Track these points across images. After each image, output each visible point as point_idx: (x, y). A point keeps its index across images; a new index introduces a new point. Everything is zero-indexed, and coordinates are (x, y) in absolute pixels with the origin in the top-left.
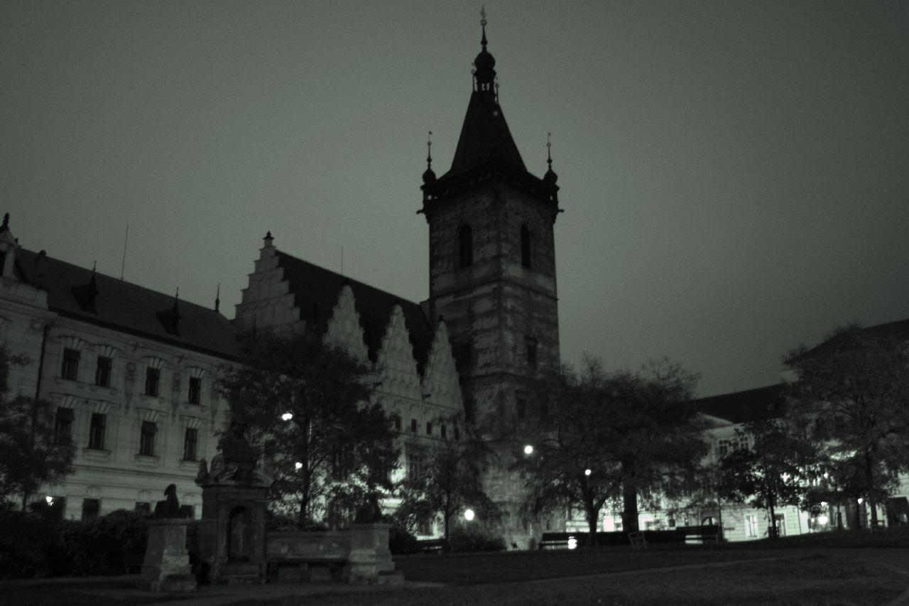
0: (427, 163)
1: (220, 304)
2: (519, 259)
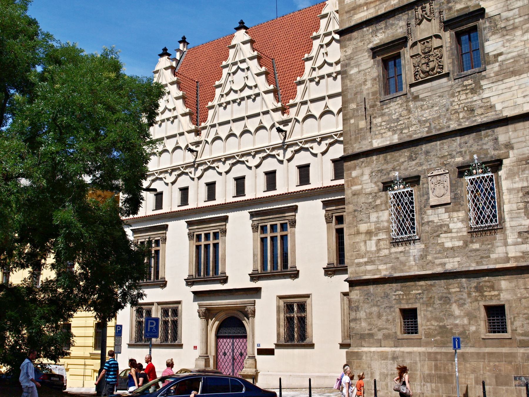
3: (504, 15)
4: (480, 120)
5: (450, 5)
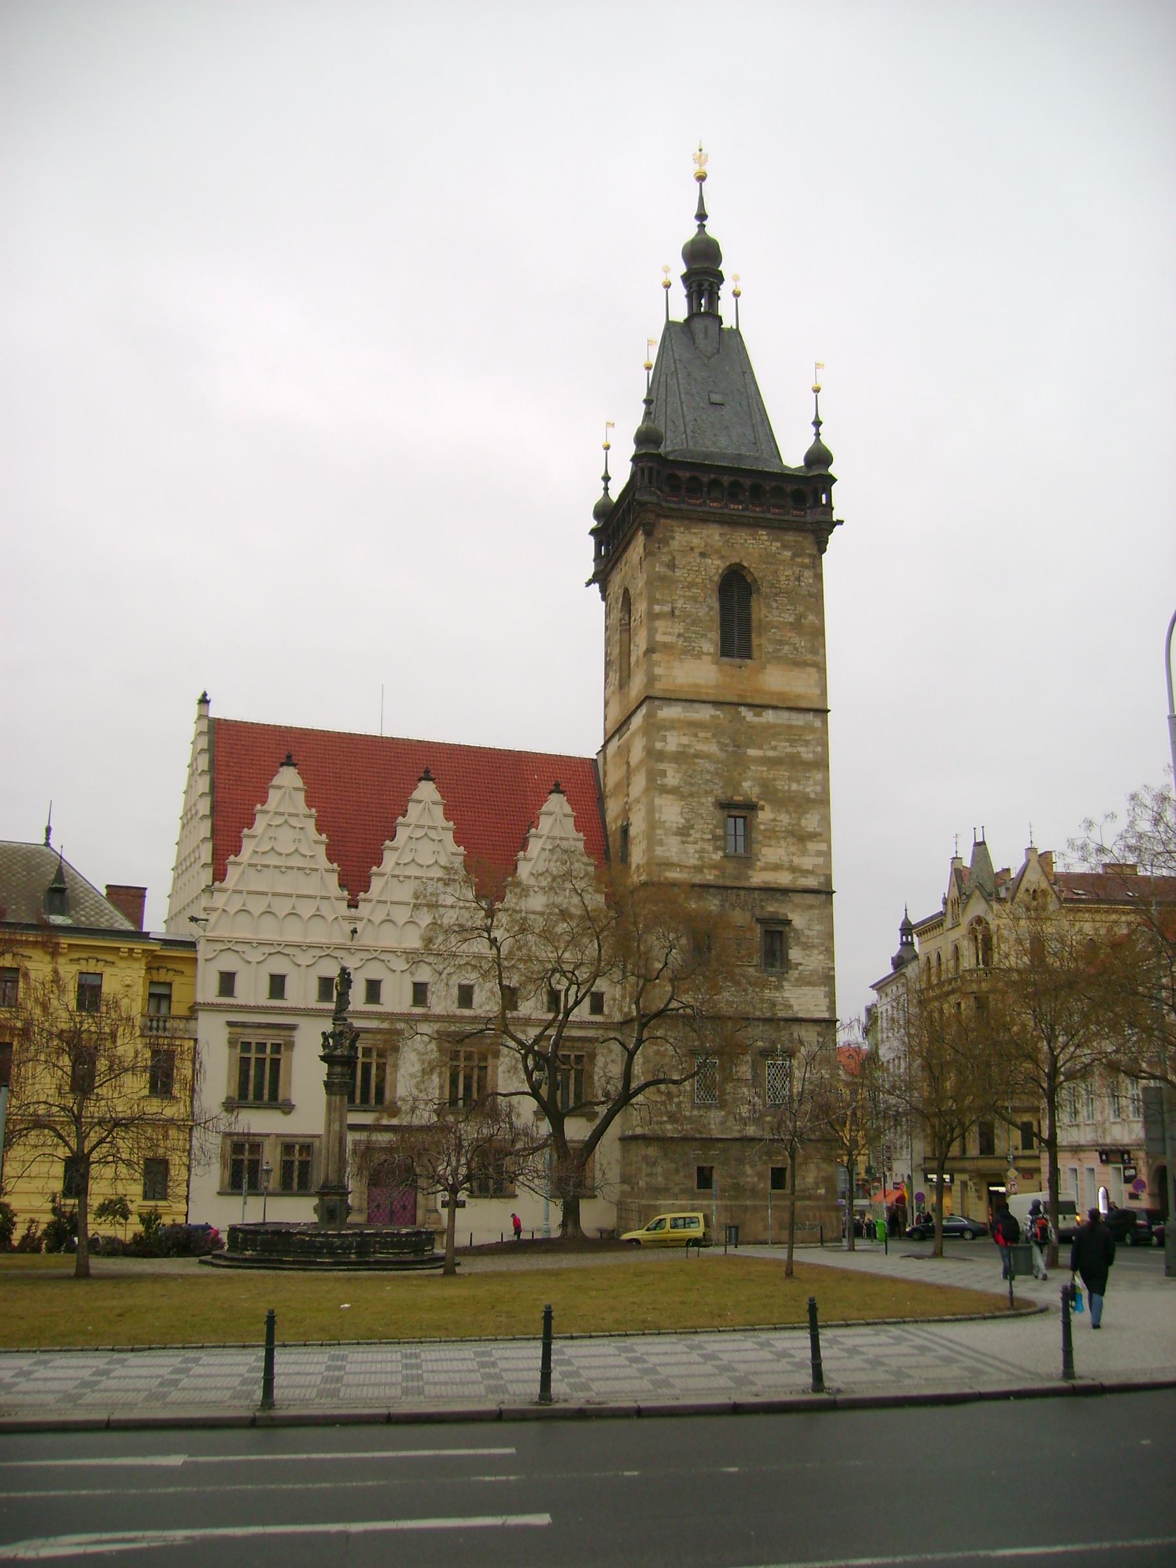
0: (603, 484)
1: (52, 833)
2: (709, 645)
3: (807, 932)
4: (781, 1014)
5: (763, 904)
